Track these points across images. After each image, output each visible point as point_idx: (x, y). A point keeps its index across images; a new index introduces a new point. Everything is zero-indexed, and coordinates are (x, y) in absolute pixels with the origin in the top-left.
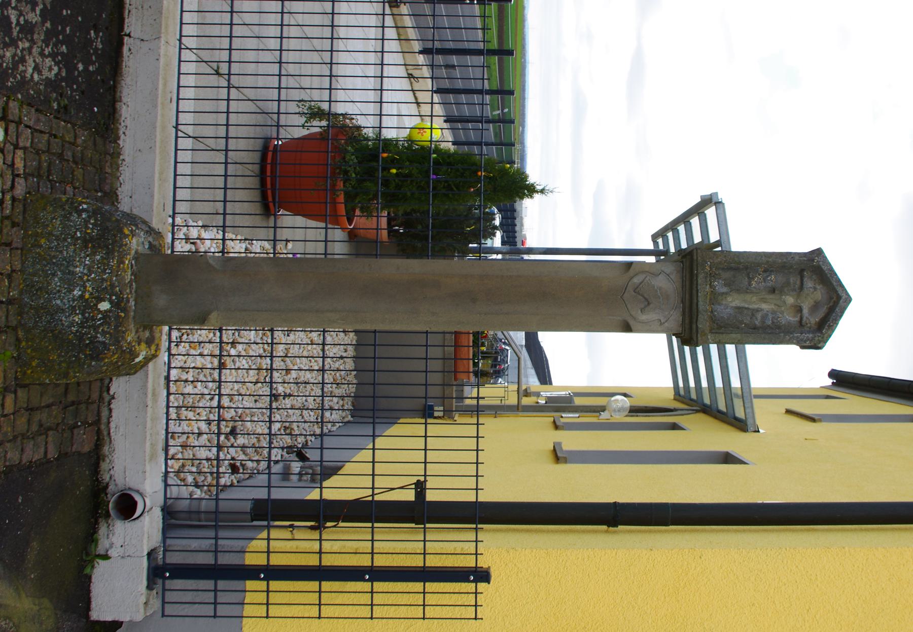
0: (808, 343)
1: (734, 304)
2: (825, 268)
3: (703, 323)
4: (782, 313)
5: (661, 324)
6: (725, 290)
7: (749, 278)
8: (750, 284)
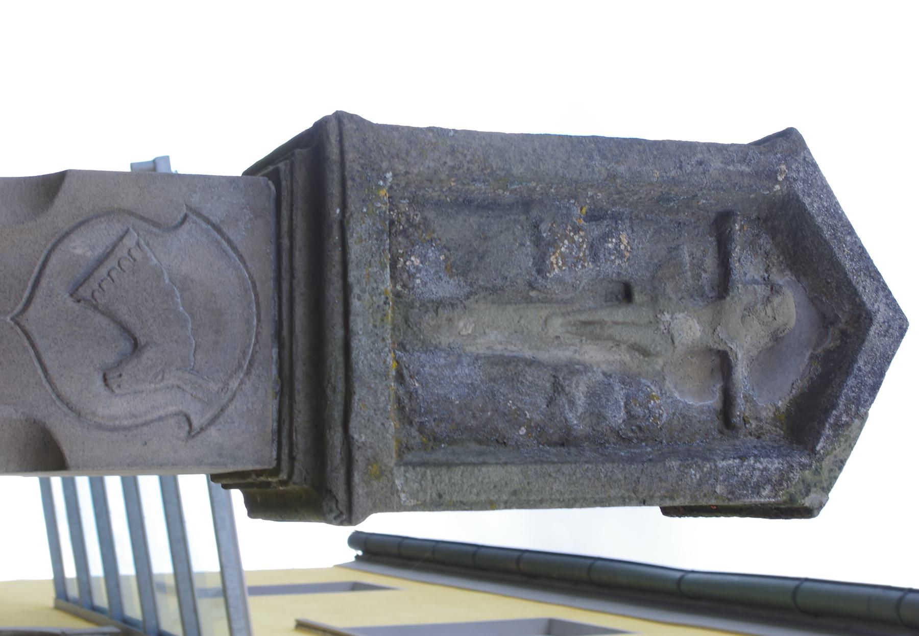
0: (766, 496)
1: (480, 346)
2: (812, 205)
3: (374, 423)
4: (659, 378)
5: (192, 433)
6: (447, 288)
7: (538, 241)
8: (541, 267)
